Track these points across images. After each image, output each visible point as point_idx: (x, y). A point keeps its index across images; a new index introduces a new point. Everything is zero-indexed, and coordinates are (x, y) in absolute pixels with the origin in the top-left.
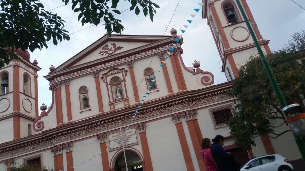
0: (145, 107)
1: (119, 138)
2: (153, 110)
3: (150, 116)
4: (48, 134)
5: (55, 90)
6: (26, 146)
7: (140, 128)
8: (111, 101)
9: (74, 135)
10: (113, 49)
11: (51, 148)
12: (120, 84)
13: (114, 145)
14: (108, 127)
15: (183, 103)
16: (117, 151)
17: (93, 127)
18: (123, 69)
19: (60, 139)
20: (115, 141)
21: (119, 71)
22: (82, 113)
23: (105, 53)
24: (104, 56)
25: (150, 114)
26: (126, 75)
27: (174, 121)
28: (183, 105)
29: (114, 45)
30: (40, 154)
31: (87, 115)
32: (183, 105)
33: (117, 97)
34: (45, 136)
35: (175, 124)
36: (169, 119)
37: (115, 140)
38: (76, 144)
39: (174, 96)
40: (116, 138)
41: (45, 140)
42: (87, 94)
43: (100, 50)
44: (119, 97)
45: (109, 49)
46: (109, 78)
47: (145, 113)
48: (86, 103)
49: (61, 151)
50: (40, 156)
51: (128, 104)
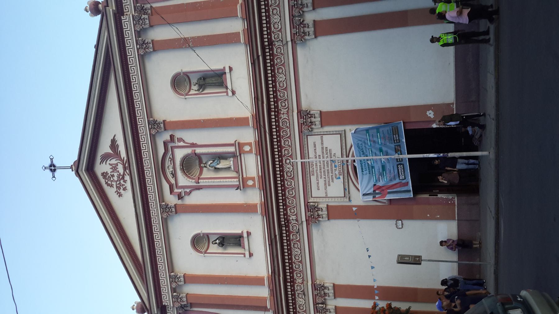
1: (323, 173)
2: (274, 87)
3: (286, 95)
5: (191, 308)
7: (311, 122)
8: (238, 183)
9: (299, 275)
10: (114, 161)
12: (199, 157)
14: (294, 197)
15: (269, 9)
18: (165, 144)
19: (302, 308)
20: (329, 185)
22: (251, 252)
23: (122, 181)
24: (128, 185)
25: (282, 95)
26: (180, 140)
27: (307, 37)
28: (273, 10)
29: (106, 157)
32: (273, 10)
33: (229, 167)
35: (316, 37)
36: (300, 51)
37: (325, 184)
39: (250, 32)
40: (322, 182)
42: (210, 236)
44: (230, 163)
45: (113, 172)
46: (183, 180)
47: (278, 105)
49: (328, 307)
51: (250, 144)
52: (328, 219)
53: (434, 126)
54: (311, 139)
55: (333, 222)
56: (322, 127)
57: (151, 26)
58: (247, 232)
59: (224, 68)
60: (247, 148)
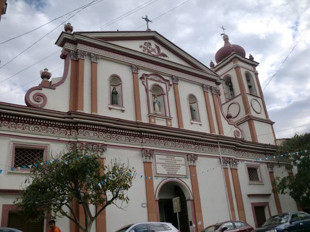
0: (202, 137)
4: (74, 119)
5: (72, 60)
6: (21, 122)
9: (109, 136)
10: (157, 51)
11: (70, 142)
12: (163, 95)
13: (161, 170)
16: (165, 178)
17: (136, 136)
18: (168, 81)
20: (162, 166)
21: (163, 81)
30: (45, 144)
31: (115, 114)
34: (66, 119)
37: (162, 163)
38: (109, 150)
40: (163, 161)
41: (59, 127)
43: (142, 43)
46: (151, 83)
48: (115, 99)
50: (44, 148)
52: (144, 162)
53: (194, 225)
54: (183, 159)
55: (143, 164)
56: (189, 166)
57: (212, 94)
58: (124, 110)
59: (200, 121)
60: (169, 123)
